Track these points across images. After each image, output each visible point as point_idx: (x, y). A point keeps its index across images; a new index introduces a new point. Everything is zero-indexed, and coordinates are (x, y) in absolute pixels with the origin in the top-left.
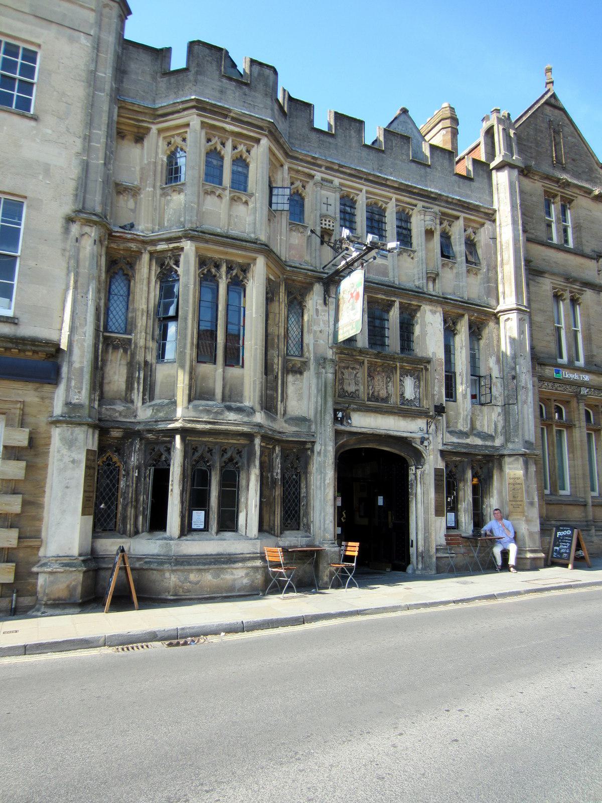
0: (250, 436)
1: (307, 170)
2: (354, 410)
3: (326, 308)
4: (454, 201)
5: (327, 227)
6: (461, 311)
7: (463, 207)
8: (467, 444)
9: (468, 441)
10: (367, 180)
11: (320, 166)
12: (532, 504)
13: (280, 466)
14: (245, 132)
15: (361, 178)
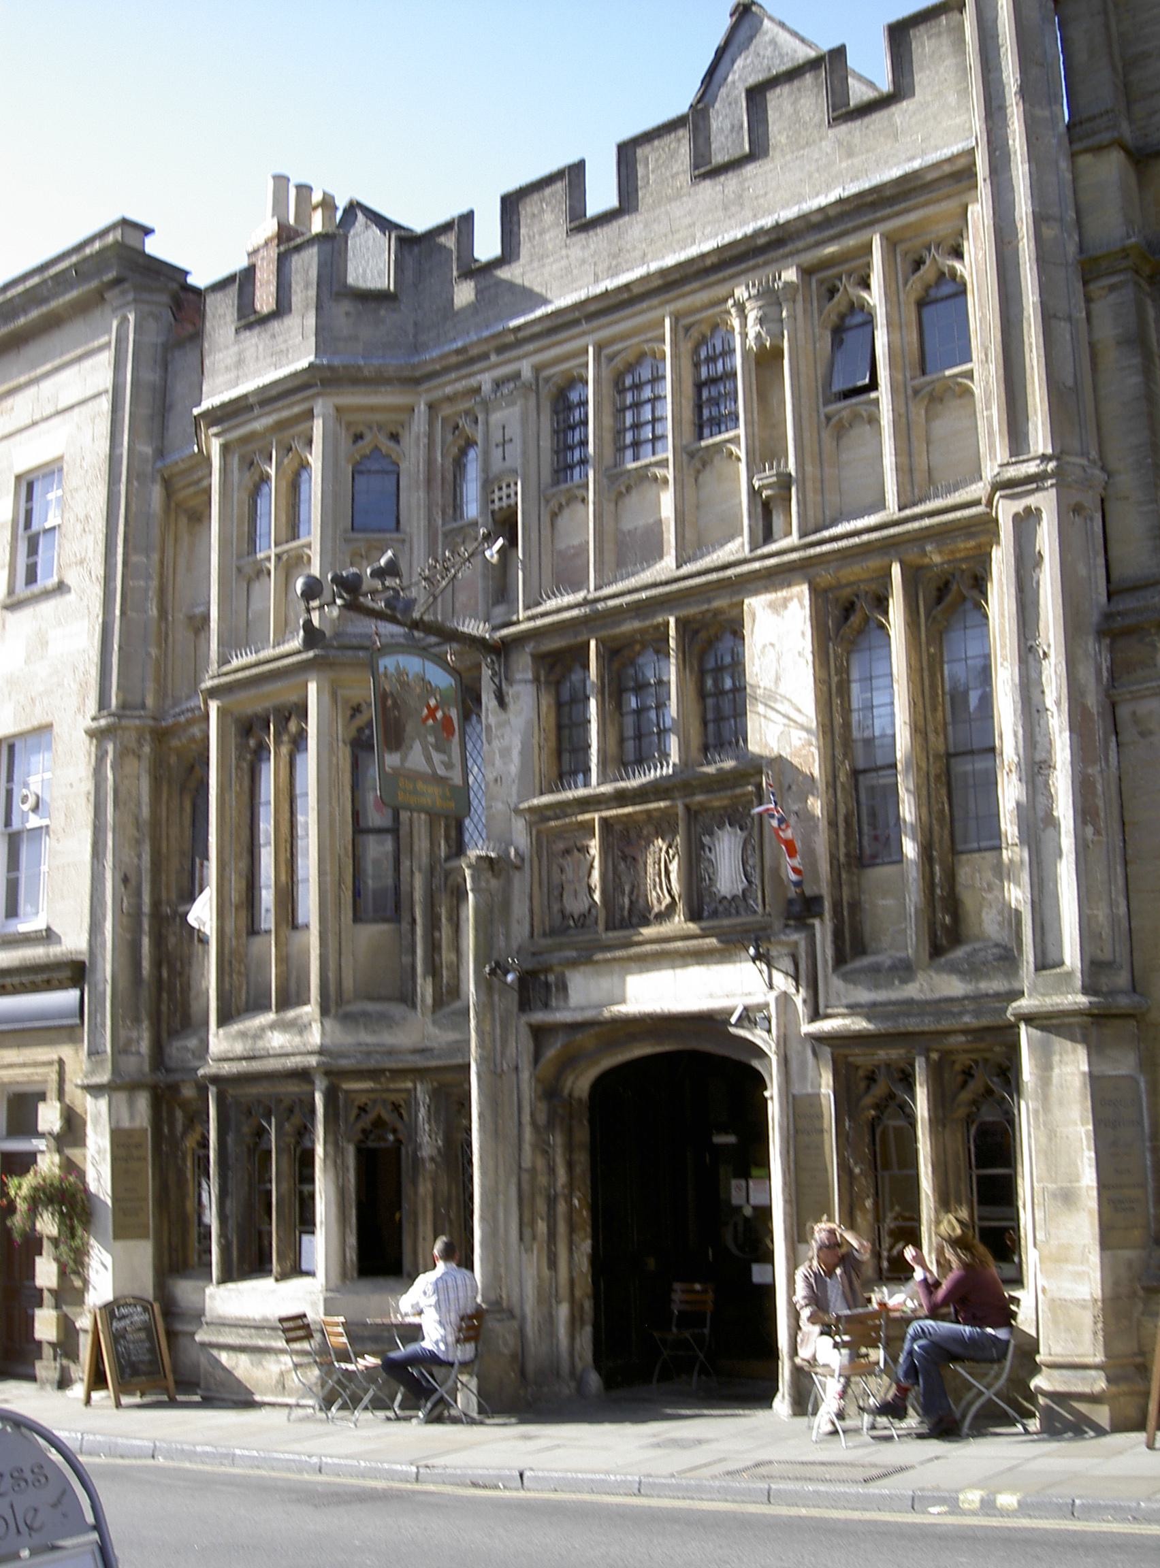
0: (303, 1075)
1: (460, 386)
2: (574, 963)
3: (503, 716)
4: (831, 212)
5: (504, 503)
6: (874, 563)
7: (874, 206)
8: (910, 1002)
9: (912, 990)
10: (590, 317)
11: (485, 356)
12: (1067, 1197)
13: (427, 1127)
14: (285, 414)
15: (576, 322)
